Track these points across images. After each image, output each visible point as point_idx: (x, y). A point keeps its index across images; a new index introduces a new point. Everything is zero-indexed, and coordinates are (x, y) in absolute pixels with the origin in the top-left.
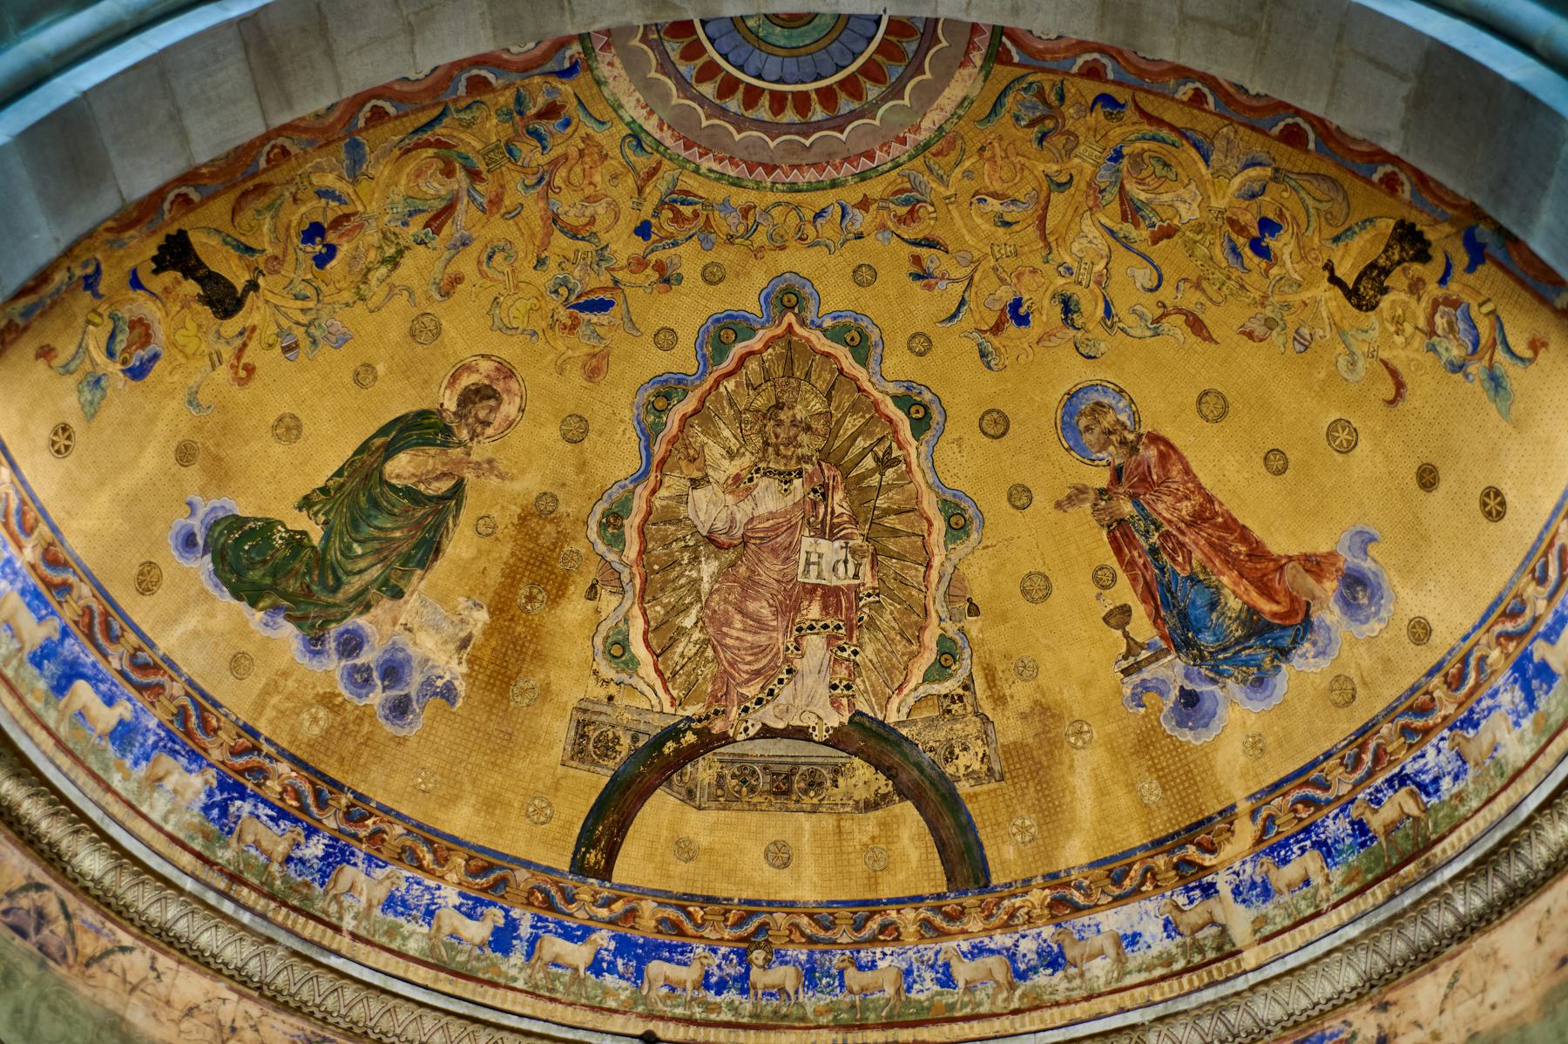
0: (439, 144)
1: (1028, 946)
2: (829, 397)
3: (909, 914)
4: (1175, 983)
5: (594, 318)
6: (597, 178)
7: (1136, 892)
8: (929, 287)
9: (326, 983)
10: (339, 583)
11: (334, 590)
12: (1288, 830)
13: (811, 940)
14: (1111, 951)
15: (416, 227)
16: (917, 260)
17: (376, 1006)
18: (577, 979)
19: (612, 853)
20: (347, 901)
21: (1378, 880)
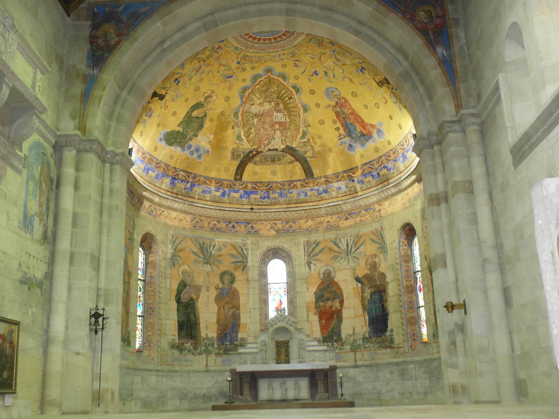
0: (198, 58)
1: (321, 189)
2: (278, 87)
3: (299, 183)
4: (347, 196)
5: (229, 79)
6: (229, 56)
7: (341, 180)
8: (298, 68)
9: (195, 208)
10: (186, 137)
11: (185, 139)
12: (367, 172)
13: (281, 188)
14: (336, 190)
15: (194, 73)
16: (295, 63)
17: (203, 210)
18: (238, 200)
19: (241, 176)
20: (196, 193)
21: (381, 184)
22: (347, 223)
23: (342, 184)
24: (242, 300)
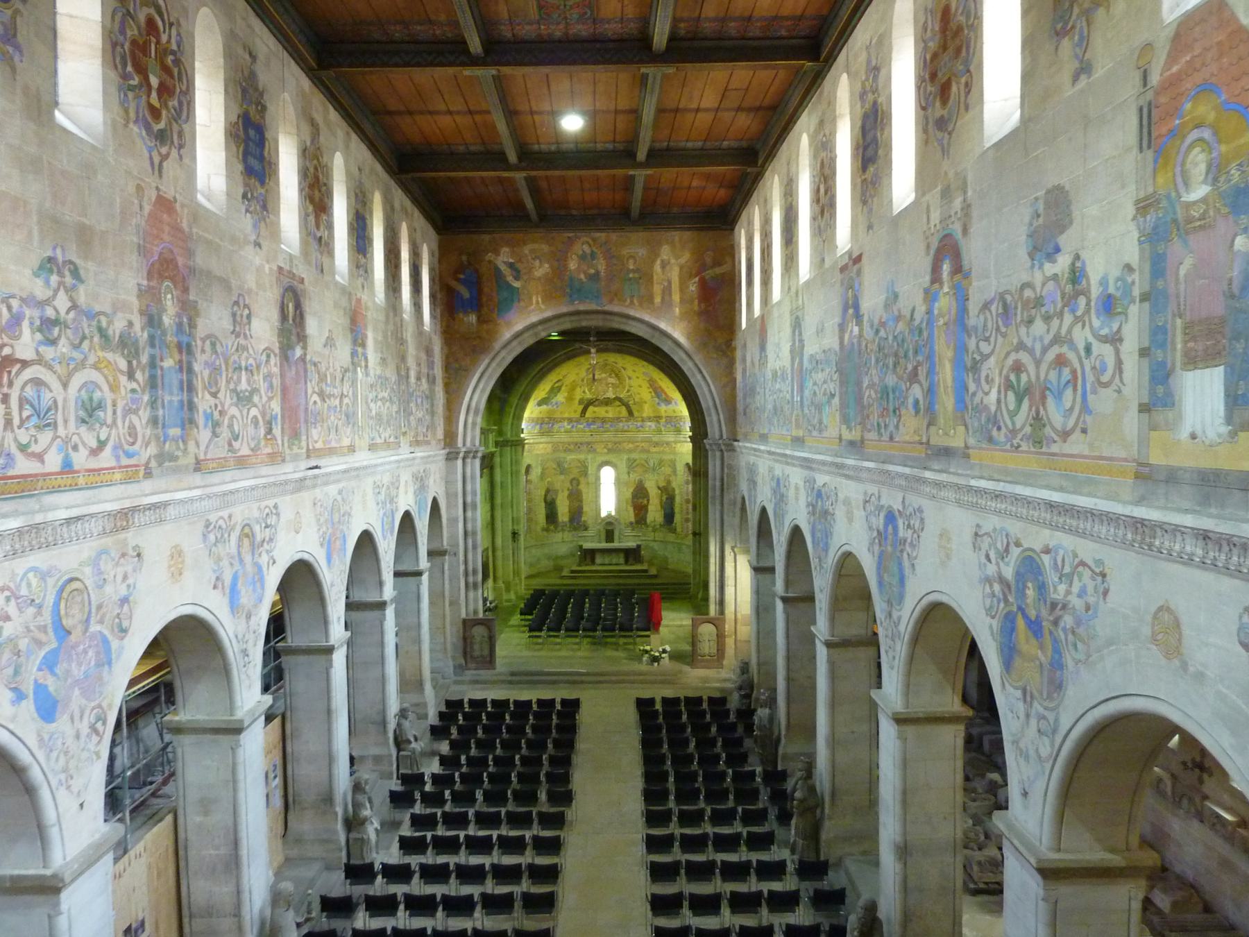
22: (654, 450)
23: (653, 425)
24: (584, 497)
